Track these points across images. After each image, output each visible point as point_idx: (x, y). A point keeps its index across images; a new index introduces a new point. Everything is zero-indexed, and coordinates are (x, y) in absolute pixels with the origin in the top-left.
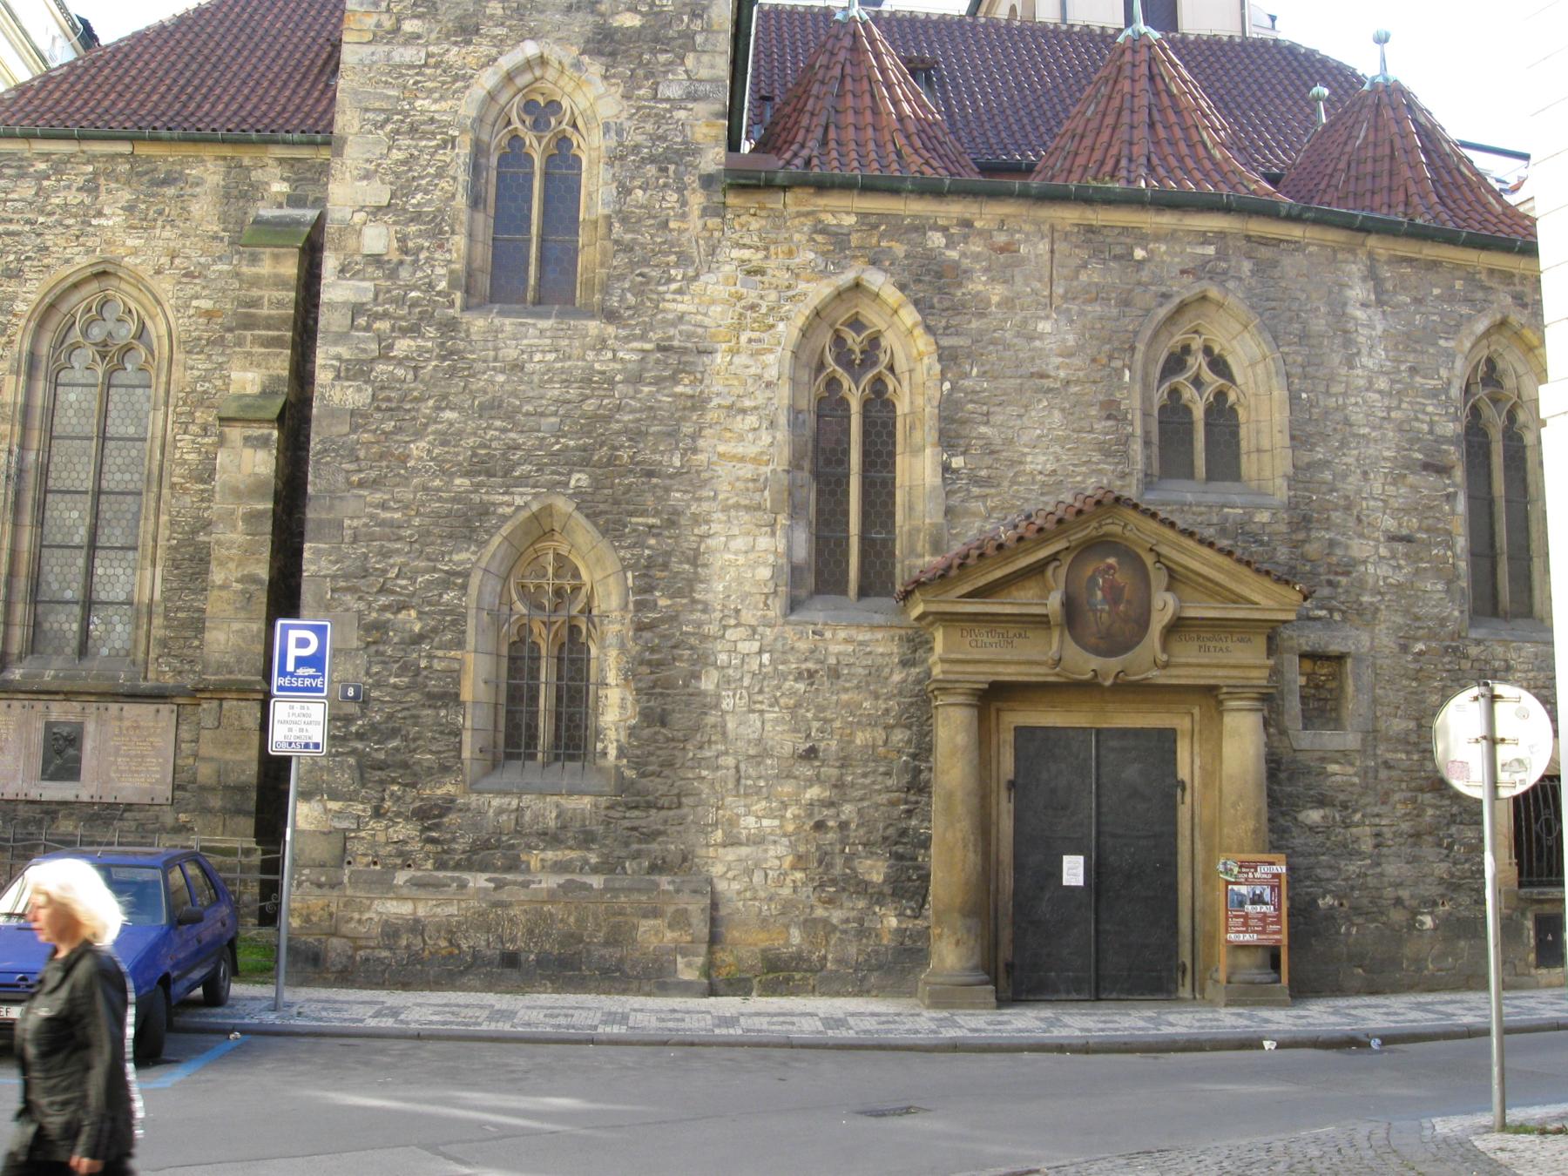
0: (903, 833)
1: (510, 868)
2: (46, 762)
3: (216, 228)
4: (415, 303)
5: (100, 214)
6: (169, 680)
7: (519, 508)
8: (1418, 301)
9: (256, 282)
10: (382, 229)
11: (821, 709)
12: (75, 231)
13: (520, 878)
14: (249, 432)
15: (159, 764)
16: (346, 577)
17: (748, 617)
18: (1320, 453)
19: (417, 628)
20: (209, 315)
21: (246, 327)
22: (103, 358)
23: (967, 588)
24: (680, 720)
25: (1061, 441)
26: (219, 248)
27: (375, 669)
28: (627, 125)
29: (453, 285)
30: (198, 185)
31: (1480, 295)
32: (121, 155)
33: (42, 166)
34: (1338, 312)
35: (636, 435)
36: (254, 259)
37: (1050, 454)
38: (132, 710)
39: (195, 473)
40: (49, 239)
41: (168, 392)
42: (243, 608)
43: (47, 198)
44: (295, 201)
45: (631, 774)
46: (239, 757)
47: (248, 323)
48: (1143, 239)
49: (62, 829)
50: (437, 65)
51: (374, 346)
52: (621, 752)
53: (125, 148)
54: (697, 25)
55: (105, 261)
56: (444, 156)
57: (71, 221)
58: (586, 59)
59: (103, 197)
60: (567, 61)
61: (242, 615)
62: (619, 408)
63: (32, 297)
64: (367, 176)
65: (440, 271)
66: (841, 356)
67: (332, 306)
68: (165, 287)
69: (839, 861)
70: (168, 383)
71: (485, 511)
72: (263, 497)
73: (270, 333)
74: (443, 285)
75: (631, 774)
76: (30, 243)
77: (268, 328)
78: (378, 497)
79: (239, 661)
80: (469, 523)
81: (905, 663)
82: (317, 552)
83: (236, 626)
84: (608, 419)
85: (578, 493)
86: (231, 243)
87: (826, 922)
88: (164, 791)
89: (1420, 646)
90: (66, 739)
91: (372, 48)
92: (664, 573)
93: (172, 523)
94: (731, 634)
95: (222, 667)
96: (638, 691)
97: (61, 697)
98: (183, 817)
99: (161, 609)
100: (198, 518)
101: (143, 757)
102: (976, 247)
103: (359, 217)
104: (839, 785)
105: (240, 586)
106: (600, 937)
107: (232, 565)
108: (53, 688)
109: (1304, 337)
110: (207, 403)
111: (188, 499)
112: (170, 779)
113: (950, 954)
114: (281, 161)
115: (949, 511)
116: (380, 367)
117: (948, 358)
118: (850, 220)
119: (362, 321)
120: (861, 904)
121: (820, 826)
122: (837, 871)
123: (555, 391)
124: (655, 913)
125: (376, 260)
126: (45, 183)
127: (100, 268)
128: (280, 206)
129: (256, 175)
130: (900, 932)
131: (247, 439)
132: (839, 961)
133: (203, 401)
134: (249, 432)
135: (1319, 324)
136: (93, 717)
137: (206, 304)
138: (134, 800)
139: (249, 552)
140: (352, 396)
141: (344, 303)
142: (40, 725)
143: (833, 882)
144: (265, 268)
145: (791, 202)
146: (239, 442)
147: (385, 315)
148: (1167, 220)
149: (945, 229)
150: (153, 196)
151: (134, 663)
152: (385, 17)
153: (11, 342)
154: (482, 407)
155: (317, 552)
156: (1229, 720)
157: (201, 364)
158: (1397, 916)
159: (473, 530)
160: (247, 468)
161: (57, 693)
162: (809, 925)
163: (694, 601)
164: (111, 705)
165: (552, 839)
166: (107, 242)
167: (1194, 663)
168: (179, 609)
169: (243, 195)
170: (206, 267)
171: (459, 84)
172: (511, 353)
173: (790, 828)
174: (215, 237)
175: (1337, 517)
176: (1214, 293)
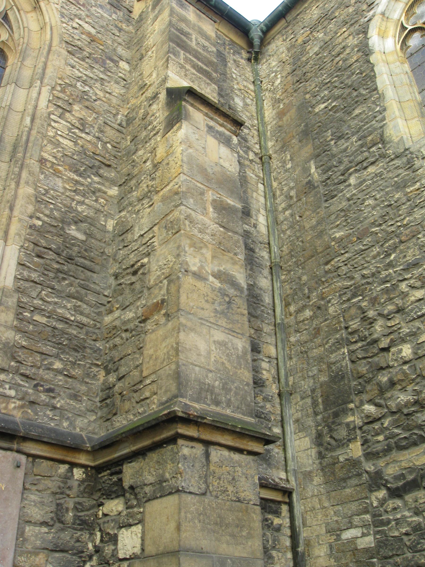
39: (69, 161)
41: (44, 69)
42: (222, 313)
46: (238, 552)
61: (223, 322)
70: (45, 64)
73: (200, 64)
79: (225, 388)
93: (38, 200)
95: (204, 391)
99: (12, 301)
105: (217, 284)
110: (87, 103)
111: (59, 183)
131: (210, 128)
134: (212, 123)
157: (81, 70)
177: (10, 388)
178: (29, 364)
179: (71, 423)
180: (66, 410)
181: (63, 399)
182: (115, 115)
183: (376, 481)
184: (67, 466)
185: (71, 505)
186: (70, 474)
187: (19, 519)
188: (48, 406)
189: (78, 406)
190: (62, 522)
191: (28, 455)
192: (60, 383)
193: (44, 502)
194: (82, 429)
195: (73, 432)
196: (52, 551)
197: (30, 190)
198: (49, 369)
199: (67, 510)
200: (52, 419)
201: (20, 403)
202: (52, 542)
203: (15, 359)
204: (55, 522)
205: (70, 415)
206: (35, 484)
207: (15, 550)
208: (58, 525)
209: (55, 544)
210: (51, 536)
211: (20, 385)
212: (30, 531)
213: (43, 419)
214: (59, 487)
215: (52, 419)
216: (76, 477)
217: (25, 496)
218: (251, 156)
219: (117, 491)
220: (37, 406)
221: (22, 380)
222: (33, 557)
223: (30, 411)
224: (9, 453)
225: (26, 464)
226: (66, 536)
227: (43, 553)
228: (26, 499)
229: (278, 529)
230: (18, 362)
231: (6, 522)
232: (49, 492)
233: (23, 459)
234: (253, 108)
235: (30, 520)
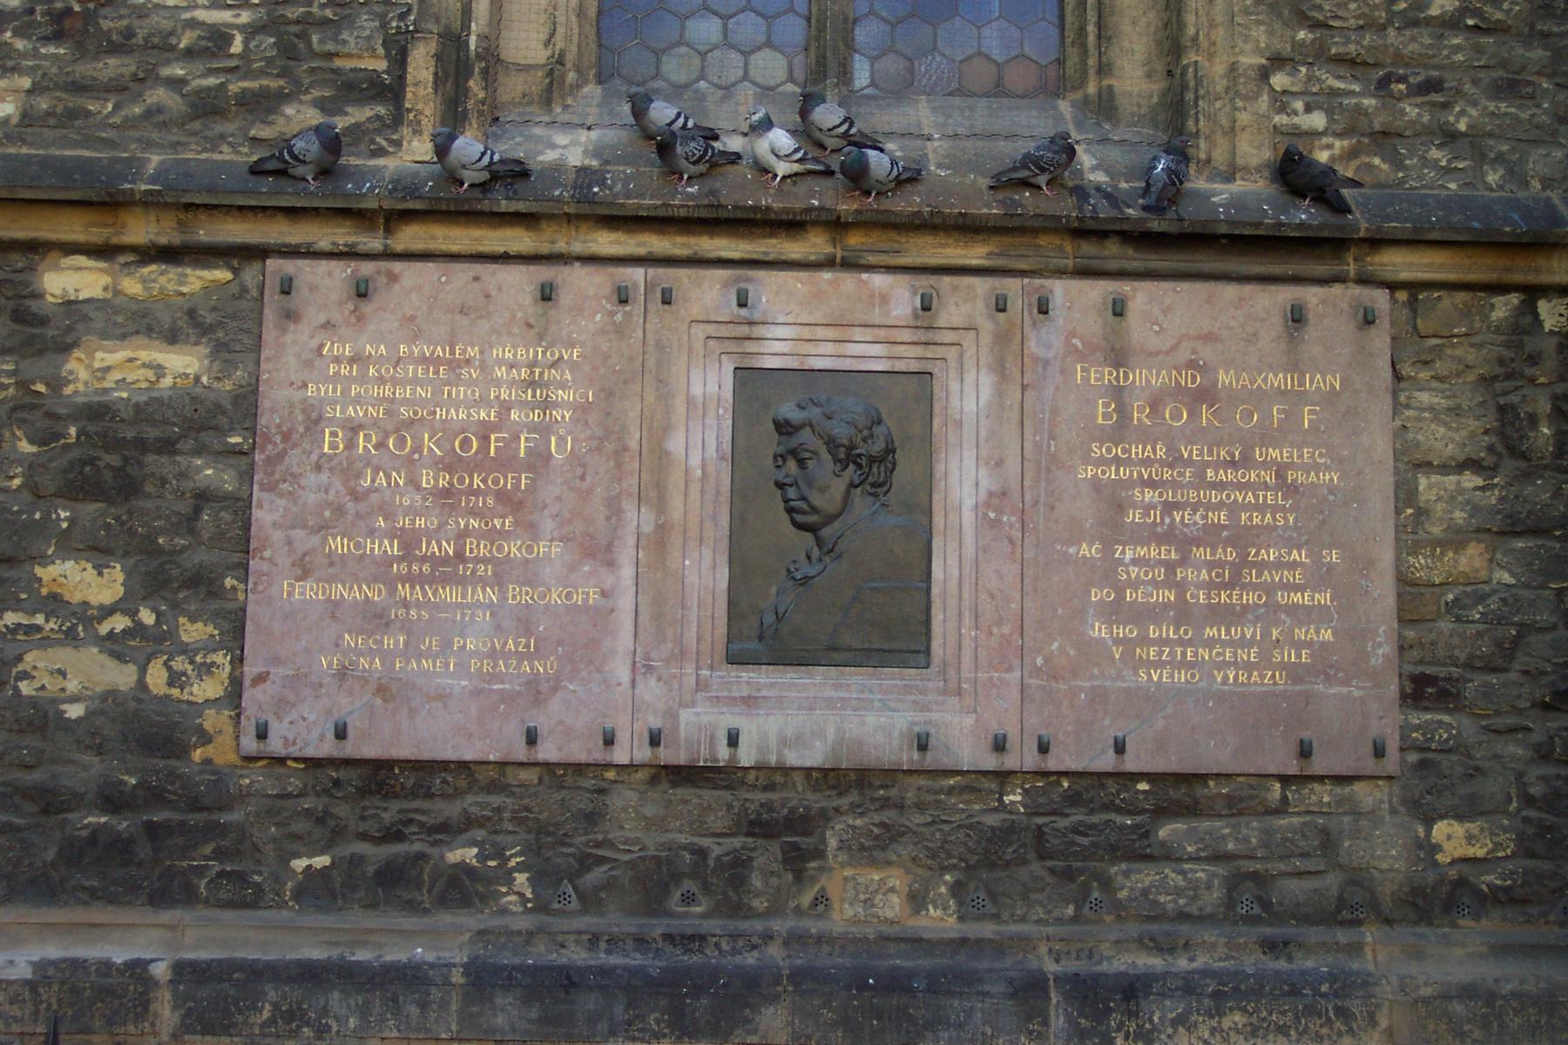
15: (1321, 577)
49: (844, 915)
88: (1363, 709)
97: (815, 244)
98: (1452, 838)
101: (1241, 538)
112: (1382, 650)
136: (979, 349)
138: (1213, 752)
142: (711, 383)
151: (1105, 107)
161: (791, 225)
164: (1060, 290)
177: (1308, 109)
178: (1352, 22)
179: (1510, 172)
180: (1491, 135)
181: (1475, 104)
184: (1514, 299)
185: (1544, 406)
186: (1527, 320)
187: (1396, 460)
188: (1432, 133)
189: (1524, 115)
190: (1524, 456)
191: (1393, 286)
192: (1460, 57)
193: (1459, 407)
194: (1547, 183)
195: (1521, 194)
196: (1501, 533)
198: (1416, 23)
199: (1533, 420)
200: (1448, 171)
201: (1346, 143)
202: (1499, 512)
203: (1308, 18)
204: (1500, 456)
205: (1505, 148)
206: (1426, 363)
207: (1397, 540)
208: (1510, 465)
209: (1506, 517)
210: (1493, 498)
211: (1334, 93)
212: (1430, 487)
213: (1420, 178)
214: (1501, 361)
215: (1448, 171)
216: (1547, 326)
217: (1402, 399)
220: (1396, 141)
221: (1339, 77)
222: (1451, 554)
223: (1377, 161)
224: (1337, 289)
225: (1392, 310)
226: (1539, 492)
227: (1479, 541)
228: (1407, 406)
230: (1316, 25)
231: (1359, 473)
232: (1472, 378)
233: (1380, 298)
235: (1429, 458)
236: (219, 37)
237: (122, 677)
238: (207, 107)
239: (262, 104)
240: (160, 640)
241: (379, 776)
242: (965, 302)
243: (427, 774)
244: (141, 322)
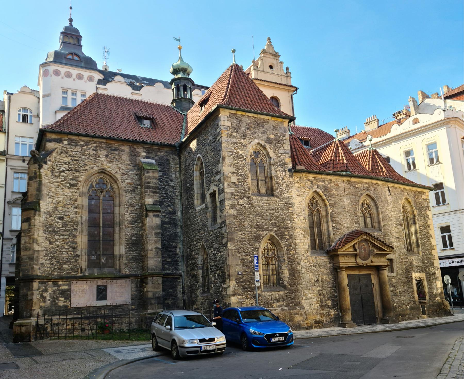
0: (333, 295)
1: (272, 307)
2: (98, 296)
3: (129, 162)
4: (242, 193)
5: (99, 157)
6: (128, 273)
7: (266, 235)
8: (395, 194)
9: (149, 178)
10: (235, 177)
11: (318, 272)
12: (93, 160)
13: (274, 309)
14: (154, 214)
16: (237, 249)
17: (305, 255)
18: (386, 223)
19: (250, 259)
20: (130, 183)
21: (148, 188)
22: (102, 192)
23: (344, 249)
24: (296, 275)
25: (349, 221)
26: (131, 168)
27: (244, 268)
28: (275, 158)
29: (249, 189)
30: (123, 151)
31: (403, 193)
32: (103, 142)
33: (82, 143)
34: (386, 198)
35: (284, 220)
36: (148, 172)
37: (348, 224)
38: (119, 281)
40: (86, 162)
43: (85, 151)
44: (147, 157)
45: (289, 286)
46: (158, 290)
47: (149, 187)
48: (357, 183)
50: (240, 143)
51: (236, 202)
52: (287, 282)
53: (104, 141)
54: (284, 138)
55: (102, 169)
56: (244, 162)
57: (92, 158)
58: (266, 144)
59: (99, 152)
60: (263, 144)
61: (156, 257)
62: (281, 215)
63: (83, 177)
64: (230, 166)
65: (246, 186)
66: (313, 204)
67: (227, 193)
68: (118, 176)
69: (324, 301)
71: (260, 235)
72: (159, 229)
74: (247, 189)
75: (289, 286)
76: (81, 163)
77: (153, 189)
78: (240, 233)
79: (156, 268)
80: (257, 238)
81: (330, 263)
82: (231, 244)
83: (155, 259)
84: (278, 217)
85: (275, 232)
86: (133, 167)
87: (323, 313)
88: (129, 301)
89: (402, 257)
90: (102, 289)
91: (227, 138)
92: (291, 246)
93: (126, 234)
94: (302, 258)
95: (153, 269)
96: (289, 270)
98: (133, 307)
99: (125, 256)
100: (132, 233)
102: (332, 184)
103: (230, 175)
104: (322, 287)
105: (155, 250)
106: (289, 320)
107: (153, 245)
108: (98, 277)
109: (382, 201)
111: (129, 229)
112: (130, 298)
113: (349, 317)
114: (143, 147)
115: (334, 234)
116: (238, 206)
117: (331, 205)
118: (313, 179)
119: (233, 196)
120: (328, 309)
121: (320, 295)
122: (324, 303)
123: (269, 211)
124: (297, 314)
125: (234, 184)
126: (84, 148)
127: (101, 171)
128: (144, 158)
129: (138, 150)
130: (334, 314)
132: (326, 321)
133: (131, 205)
134: (154, 214)
135: (383, 199)
137: (129, 181)
138: (122, 304)
139: (156, 242)
140: (233, 212)
141: (229, 193)
143: (323, 306)
144: (151, 174)
145: (304, 175)
146: (152, 216)
147: (237, 195)
148: (360, 180)
149: (327, 181)
150: (113, 153)
151: (116, 269)
152: (229, 132)
153: (79, 188)
154: (257, 215)
155: (231, 244)
156: (382, 272)
157: (129, 196)
158: (404, 306)
159: (258, 239)
160: (154, 222)
162: (321, 314)
163: (296, 252)
165: (278, 301)
166: (101, 164)
167: (377, 261)
168: (129, 256)
169: (135, 155)
170: (128, 172)
171: (244, 148)
172: (260, 204)
173: (316, 295)
174: (129, 165)
175: (389, 234)
176: (369, 193)
182: (138, 205)
183: (190, 275)
197: (124, 233)
218: (177, 194)
219: (144, 283)
229: (179, 282)
234: (178, 175)
236: (68, 269)
237: (64, 304)
238: (68, 273)
239: (71, 273)
240: (66, 302)
241: (78, 308)
242: (109, 281)
243: (81, 308)
244: (64, 285)
